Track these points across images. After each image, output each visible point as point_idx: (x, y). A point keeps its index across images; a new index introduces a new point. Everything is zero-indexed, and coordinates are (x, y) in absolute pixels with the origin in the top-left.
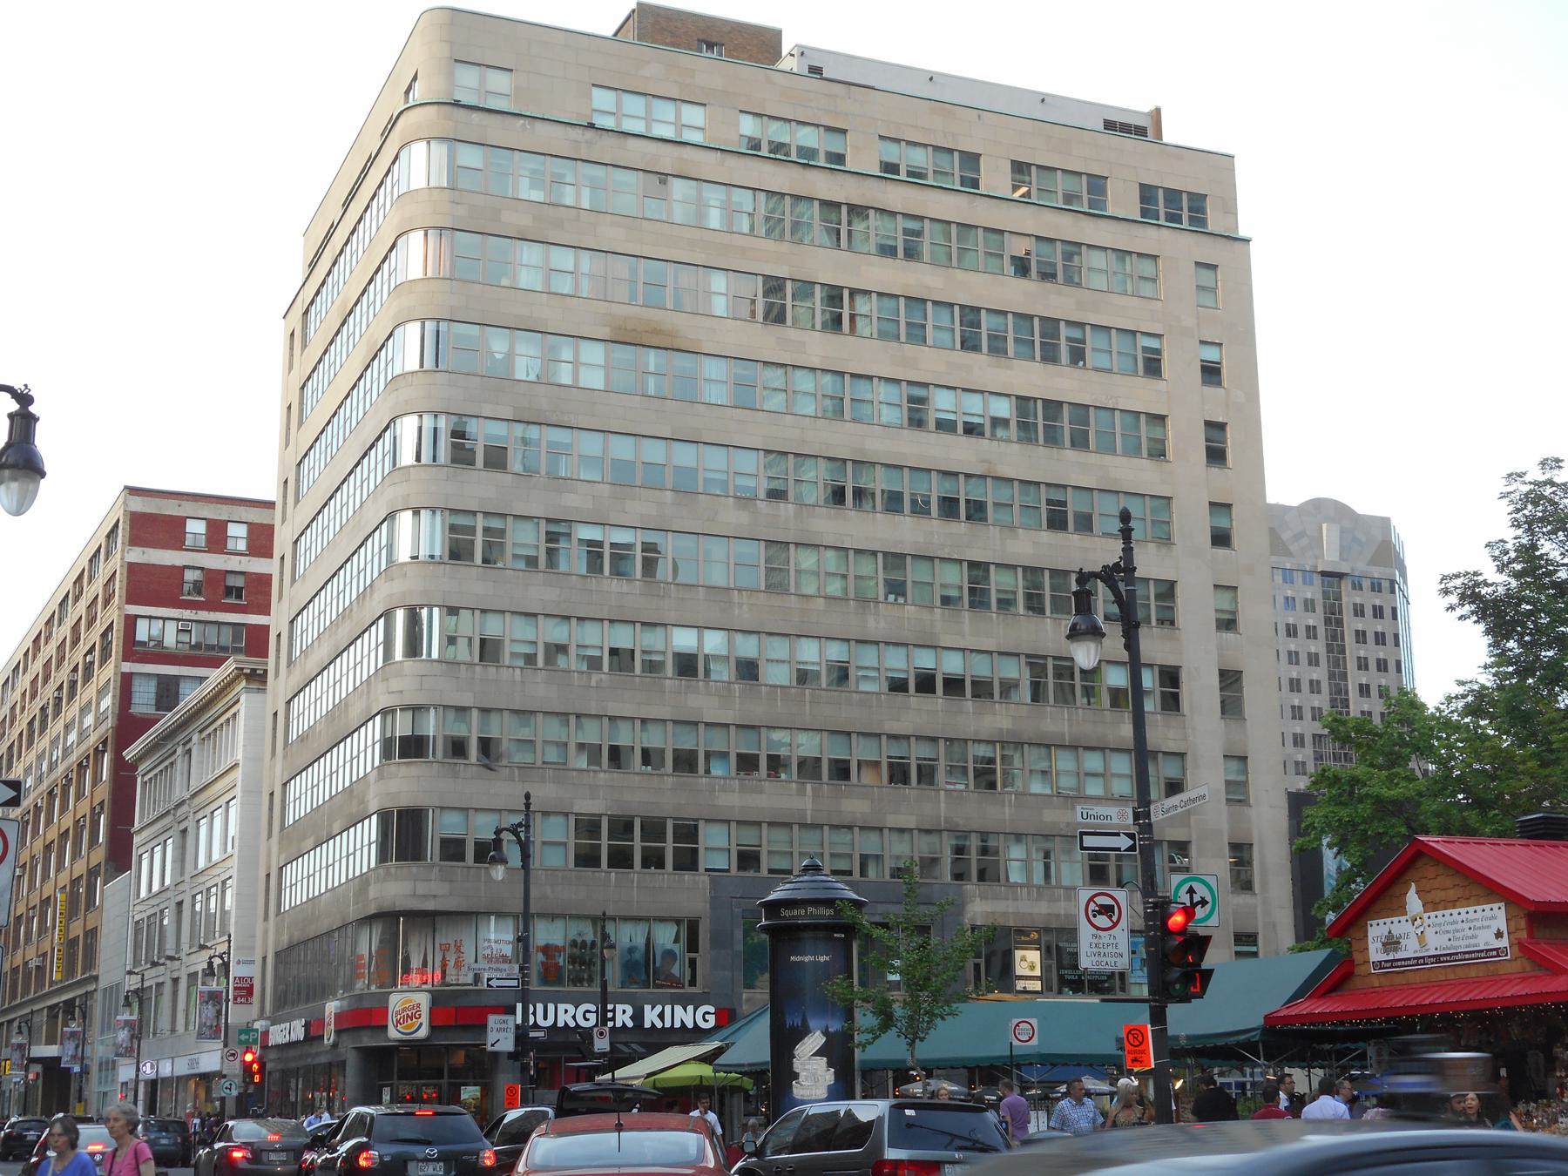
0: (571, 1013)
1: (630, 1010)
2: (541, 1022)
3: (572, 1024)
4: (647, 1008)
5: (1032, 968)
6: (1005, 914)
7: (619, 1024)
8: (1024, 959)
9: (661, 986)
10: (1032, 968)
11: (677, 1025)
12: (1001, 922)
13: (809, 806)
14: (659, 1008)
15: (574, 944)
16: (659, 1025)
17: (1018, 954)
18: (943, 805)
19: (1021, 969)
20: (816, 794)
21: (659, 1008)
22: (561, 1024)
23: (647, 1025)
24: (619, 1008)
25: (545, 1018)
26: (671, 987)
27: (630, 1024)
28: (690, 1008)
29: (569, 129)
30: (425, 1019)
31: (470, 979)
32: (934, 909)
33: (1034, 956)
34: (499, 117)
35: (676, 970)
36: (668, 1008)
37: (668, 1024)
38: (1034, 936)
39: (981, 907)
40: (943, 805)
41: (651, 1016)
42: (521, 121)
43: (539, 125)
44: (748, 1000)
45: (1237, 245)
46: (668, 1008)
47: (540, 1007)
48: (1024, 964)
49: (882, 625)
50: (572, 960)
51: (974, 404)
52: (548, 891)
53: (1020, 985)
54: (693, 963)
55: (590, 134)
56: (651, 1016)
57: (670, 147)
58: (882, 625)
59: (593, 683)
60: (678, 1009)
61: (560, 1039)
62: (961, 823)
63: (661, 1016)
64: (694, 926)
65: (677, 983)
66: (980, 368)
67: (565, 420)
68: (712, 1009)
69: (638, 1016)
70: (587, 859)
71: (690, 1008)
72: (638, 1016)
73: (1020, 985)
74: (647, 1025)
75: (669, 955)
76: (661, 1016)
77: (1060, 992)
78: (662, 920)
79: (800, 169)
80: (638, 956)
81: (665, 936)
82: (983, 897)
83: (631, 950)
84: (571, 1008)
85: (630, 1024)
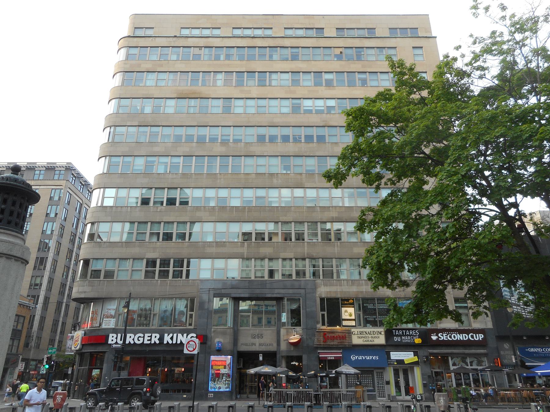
0: (132, 338)
1: (158, 336)
2: (119, 341)
3: (132, 342)
4: (166, 335)
5: (351, 315)
6: (336, 292)
7: (153, 342)
8: (346, 311)
9: (176, 326)
10: (351, 315)
11: (179, 342)
12: (333, 295)
13: (246, 251)
14: (171, 335)
15: (142, 310)
16: (170, 342)
17: (343, 309)
18: (306, 248)
19: (345, 316)
20: (248, 246)
21: (171, 335)
22: (127, 342)
23: (165, 342)
24: (154, 335)
25: (121, 340)
26: (181, 326)
27: (158, 342)
28: (185, 335)
29: (168, 38)
30: (79, 342)
31: (98, 325)
32: (302, 291)
33: (351, 310)
34: (144, 38)
35: (184, 319)
36: (175, 335)
37: (174, 342)
38: (351, 301)
39: (324, 290)
40: (306, 248)
41: (167, 339)
42: (151, 38)
43: (157, 39)
44: (214, 331)
45: (430, 39)
46: (175, 335)
47: (119, 335)
48: (346, 314)
49: (280, 181)
50: (140, 316)
51: (320, 103)
52: (132, 288)
53: (344, 323)
54: (191, 316)
55: (175, 39)
56: (167, 339)
57: (203, 39)
58: (280, 181)
59: (159, 210)
60: (180, 335)
61: (129, 349)
62: (315, 255)
63: (172, 338)
64: (192, 301)
65: (182, 324)
66: (323, 91)
67: (157, 124)
68: (195, 335)
69: (161, 339)
70: (149, 274)
71: (185, 335)
72: (161, 339)
73: (344, 323)
74: (165, 342)
75: (181, 313)
76: (172, 338)
77: (365, 326)
78: (180, 298)
79: (251, 39)
80: (168, 314)
81: (181, 305)
82: (325, 285)
83: (165, 311)
84: (132, 335)
85: (158, 342)
